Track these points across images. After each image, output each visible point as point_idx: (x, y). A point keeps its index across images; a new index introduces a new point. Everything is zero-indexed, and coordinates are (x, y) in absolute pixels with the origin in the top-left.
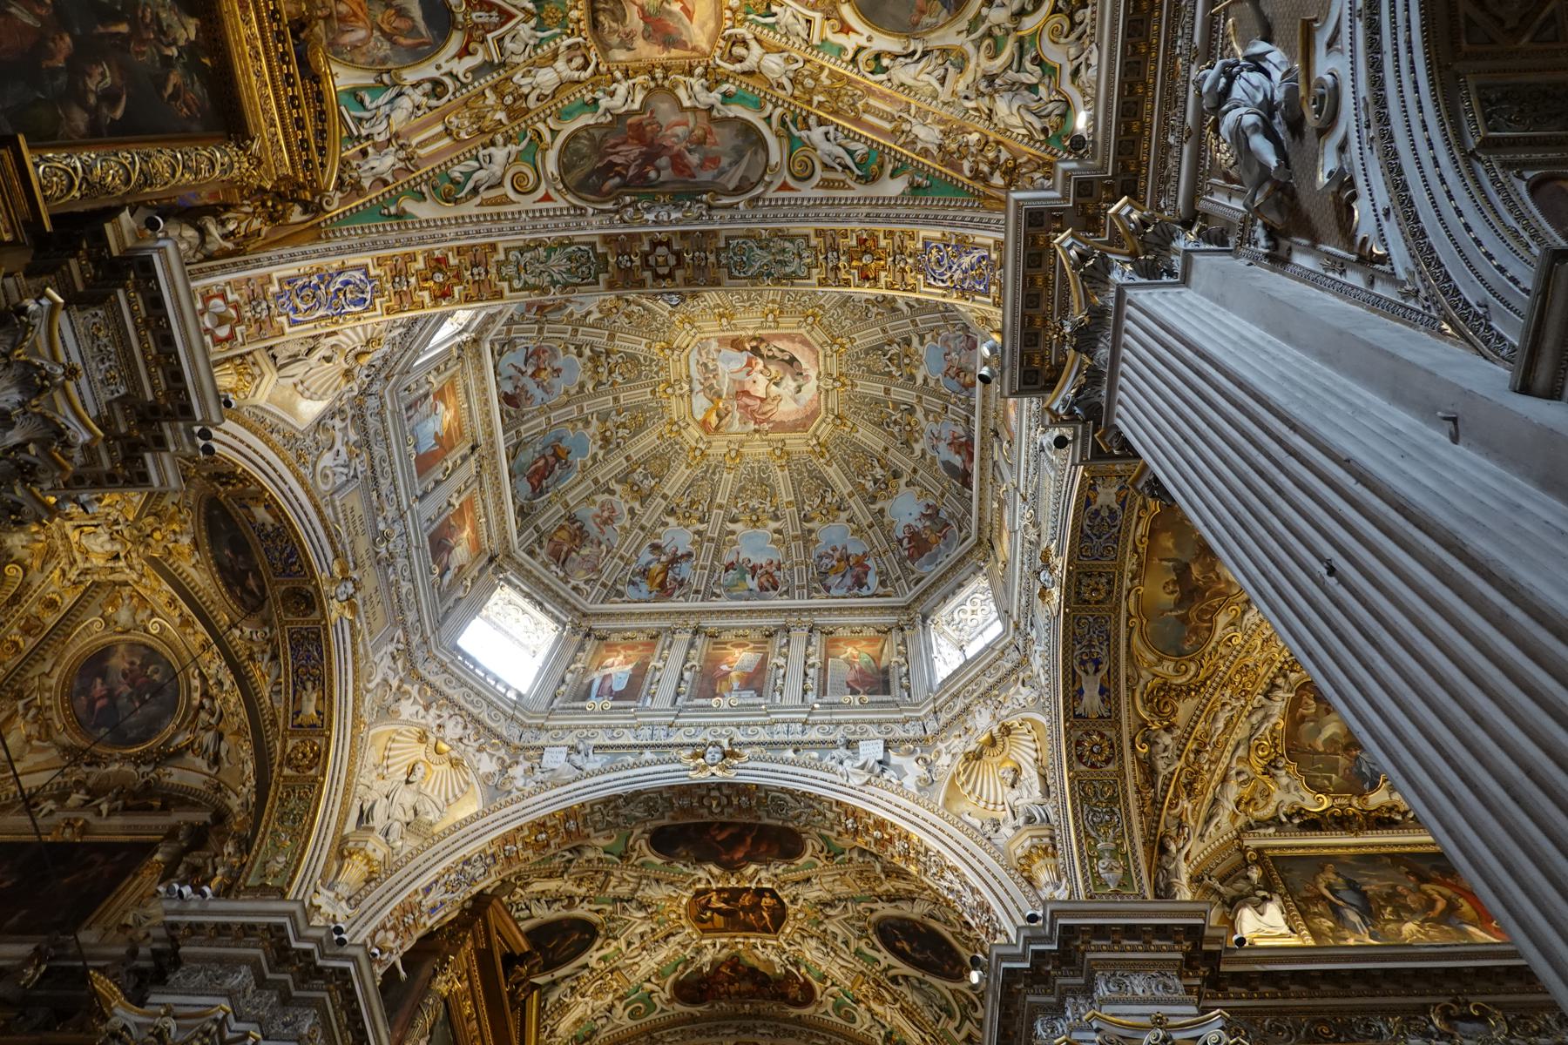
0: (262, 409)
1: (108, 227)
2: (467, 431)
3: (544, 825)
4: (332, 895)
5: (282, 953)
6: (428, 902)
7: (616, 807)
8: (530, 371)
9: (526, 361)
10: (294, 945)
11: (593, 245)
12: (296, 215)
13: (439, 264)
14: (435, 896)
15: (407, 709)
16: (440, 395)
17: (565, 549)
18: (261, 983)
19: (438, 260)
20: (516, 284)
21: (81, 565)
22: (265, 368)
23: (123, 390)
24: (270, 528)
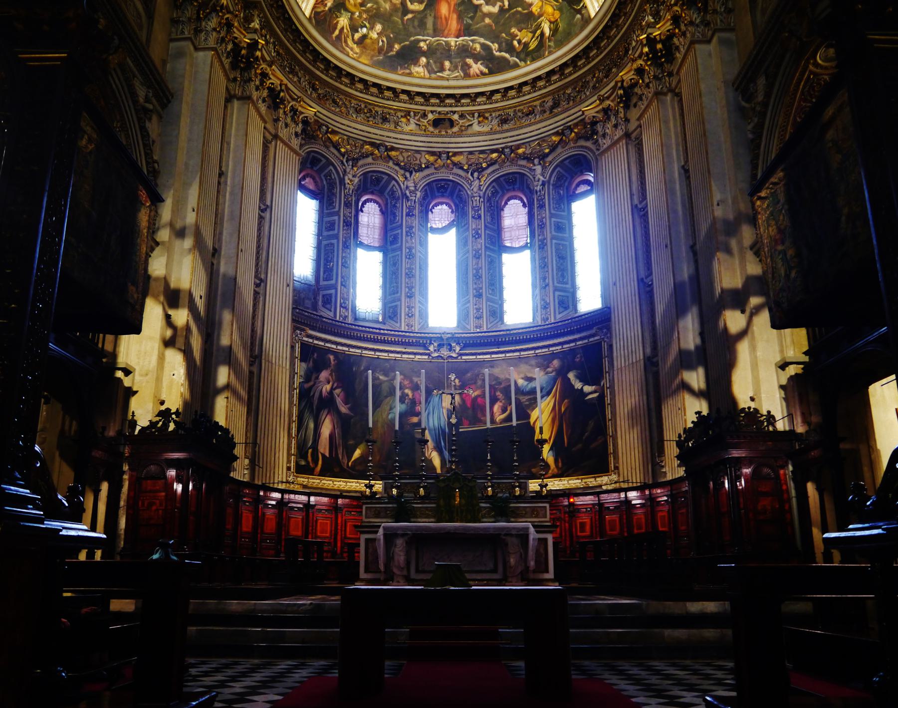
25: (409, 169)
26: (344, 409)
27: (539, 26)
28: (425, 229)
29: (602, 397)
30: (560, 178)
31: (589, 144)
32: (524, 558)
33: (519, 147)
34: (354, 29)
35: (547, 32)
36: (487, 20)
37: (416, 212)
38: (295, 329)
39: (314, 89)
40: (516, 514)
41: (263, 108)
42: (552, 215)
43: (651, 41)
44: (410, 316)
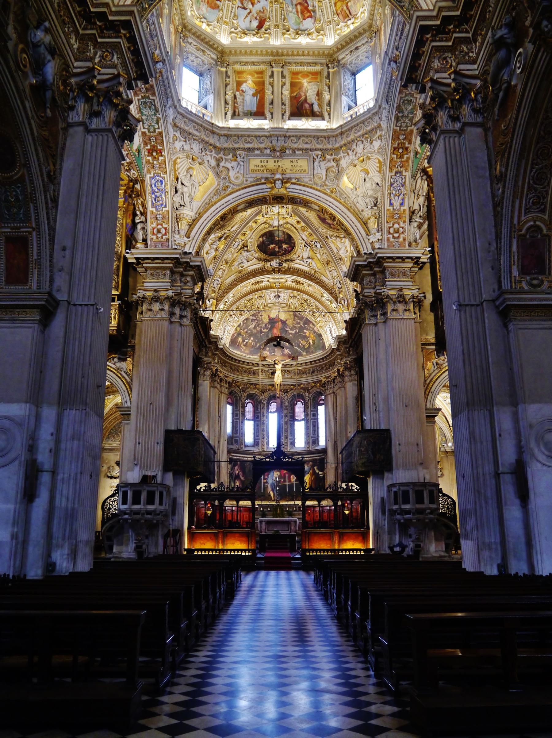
0: (203, 203)
1: (130, 261)
2: (261, 67)
3: (395, 149)
4: (372, 236)
5: (369, 266)
6: (396, 205)
7: (402, 117)
8: (250, 6)
9: (245, 8)
10: (366, 263)
11: (139, 100)
12: (138, 187)
13: (150, 152)
14: (396, 203)
15: (344, 163)
16: (239, 84)
17: (345, 8)
18: (374, 275)
19: (149, 152)
20: (156, 126)
21: (285, 214)
22: (181, 212)
23: (169, 272)
24: (247, 205)
25: (263, 392)
26: (242, 478)
27: (308, 340)
28: (268, 412)
29: (324, 476)
30: (314, 397)
31: (323, 389)
32: (295, 527)
33: (301, 384)
34: (243, 341)
35: (311, 343)
36: (291, 335)
37: (265, 407)
38: (228, 454)
39: (231, 368)
40: (294, 515)
41: (218, 386)
42: (311, 411)
43: (338, 370)
44: (263, 445)
